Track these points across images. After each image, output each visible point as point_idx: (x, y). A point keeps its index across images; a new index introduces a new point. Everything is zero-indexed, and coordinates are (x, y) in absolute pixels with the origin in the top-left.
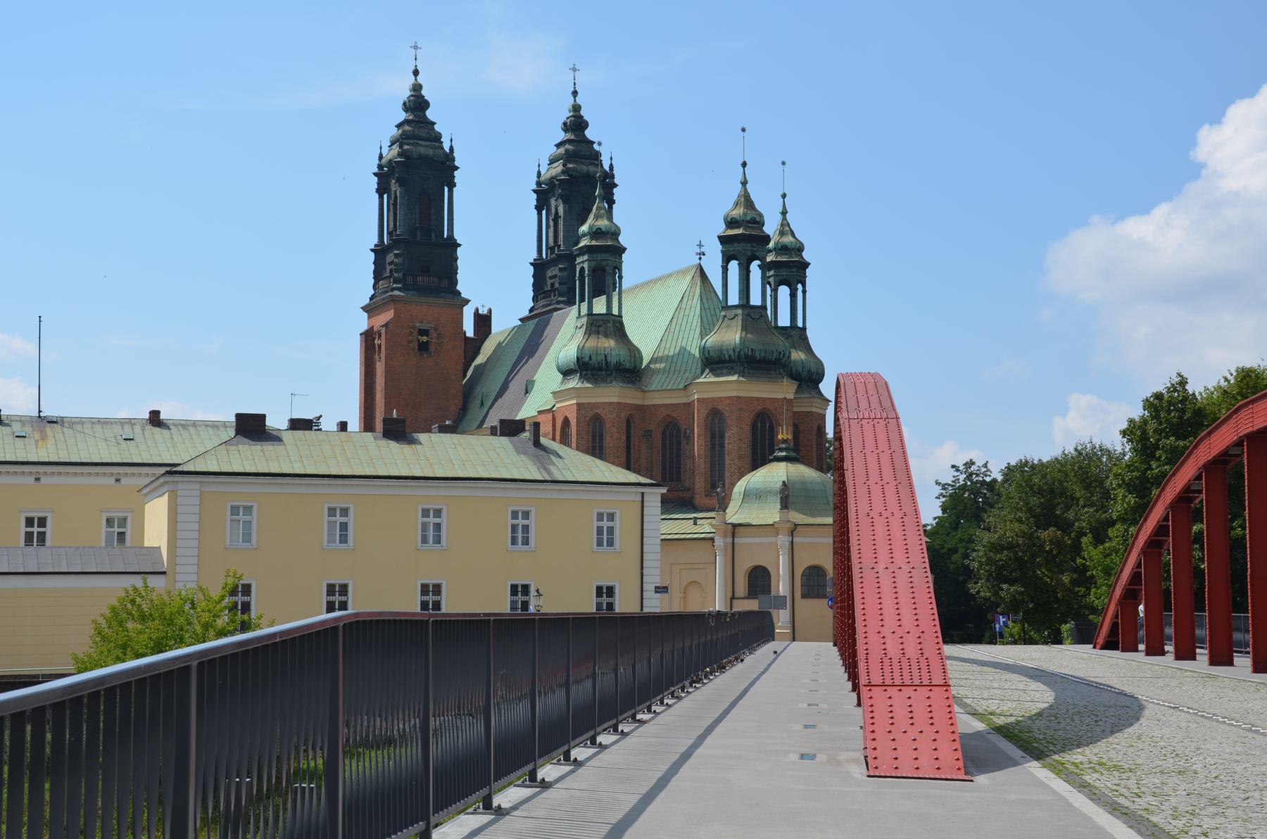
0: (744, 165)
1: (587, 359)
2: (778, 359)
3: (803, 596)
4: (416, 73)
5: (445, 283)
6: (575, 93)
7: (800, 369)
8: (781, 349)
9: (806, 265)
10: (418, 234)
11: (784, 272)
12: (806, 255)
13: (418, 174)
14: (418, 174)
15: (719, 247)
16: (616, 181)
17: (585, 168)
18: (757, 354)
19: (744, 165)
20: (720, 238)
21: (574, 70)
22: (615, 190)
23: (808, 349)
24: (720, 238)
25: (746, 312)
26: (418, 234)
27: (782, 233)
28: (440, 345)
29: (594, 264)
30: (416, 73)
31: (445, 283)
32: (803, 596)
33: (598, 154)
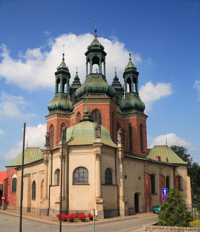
1: (50, 107)
3: (74, 184)
4: (77, 73)
6: (116, 73)
8: (104, 86)
9: (137, 74)
12: (137, 71)
15: (86, 57)
17: (116, 87)
18: (93, 88)
20: (85, 54)
23: (139, 99)
24: (85, 54)
25: (92, 76)
27: (129, 65)
29: (57, 78)
30: (77, 73)
32: (74, 184)
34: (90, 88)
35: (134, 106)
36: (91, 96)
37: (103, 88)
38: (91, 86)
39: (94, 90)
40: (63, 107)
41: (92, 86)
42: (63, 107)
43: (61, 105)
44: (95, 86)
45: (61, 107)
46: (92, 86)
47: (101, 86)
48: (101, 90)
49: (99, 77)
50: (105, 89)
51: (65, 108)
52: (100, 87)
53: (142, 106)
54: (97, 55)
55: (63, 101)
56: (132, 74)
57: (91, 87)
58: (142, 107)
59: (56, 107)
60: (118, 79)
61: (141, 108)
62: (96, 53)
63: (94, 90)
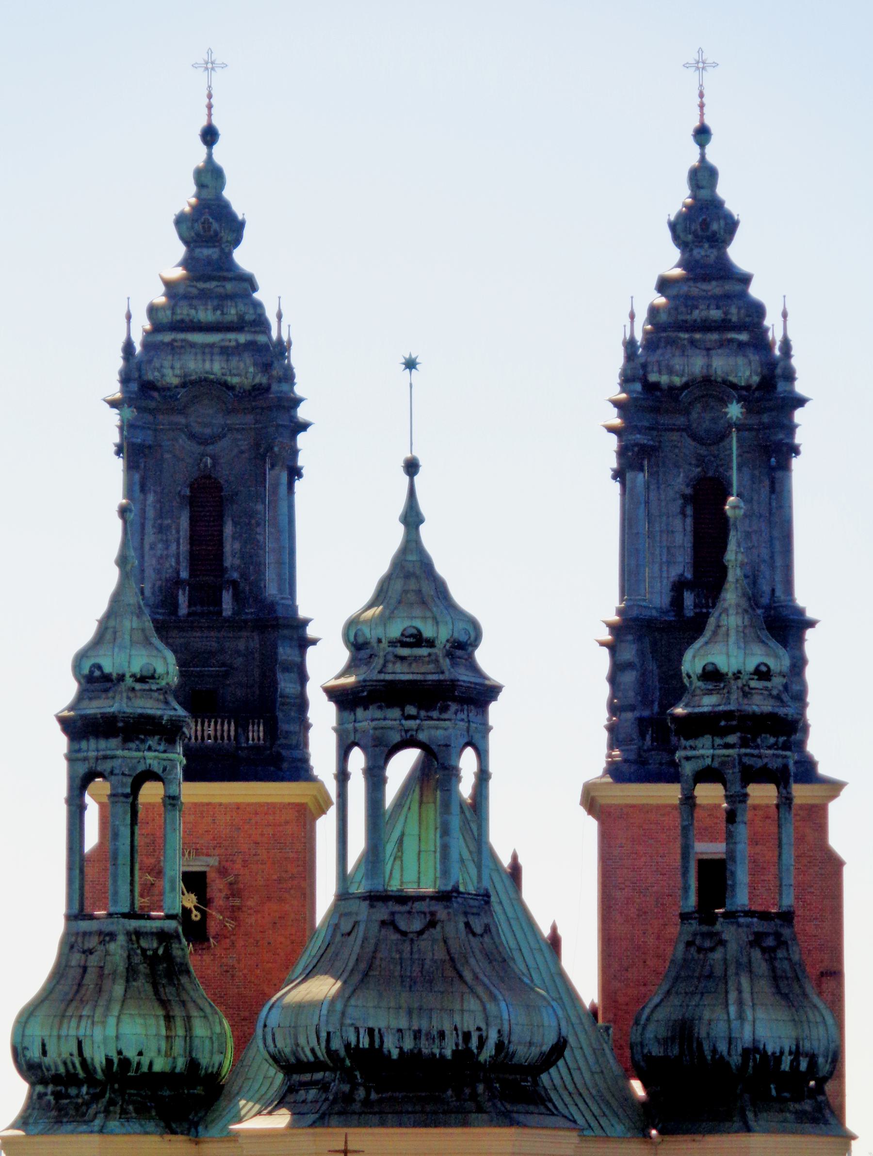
0: (412, 467)
1: (35, 1053)
2: (464, 1056)
4: (210, 136)
5: (256, 733)
6: (702, 134)
7: (722, 1047)
8: (469, 1024)
10: (183, 599)
11: (705, 750)
13: (209, 420)
14: (209, 420)
16: (800, 387)
19: (412, 467)
21: (701, 65)
22: (799, 415)
25: (382, 912)
26: (183, 599)
28: (234, 912)
30: (210, 136)
31: (256, 733)
33: (757, 310)
34: (365, 1042)
35: (735, 1060)
36: (374, 1096)
37: (467, 1036)
38: (371, 1026)
39: (395, 1054)
40: (145, 1061)
41: (380, 1020)
42: (145, 1061)
43: (131, 1053)
44: (403, 1024)
45: (125, 1062)
46: (382, 1024)
47: (447, 1027)
48: (448, 1053)
49: (432, 924)
50: (482, 1042)
51: (157, 1068)
52: (442, 1034)
53: (807, 1046)
54: (419, 729)
55: (152, 1021)
56: (732, 739)
57: (371, 1031)
58: (813, 1058)
59: (84, 1062)
60: (731, 225)
61: (804, 1065)
62: (411, 710)
63: (395, 1054)
